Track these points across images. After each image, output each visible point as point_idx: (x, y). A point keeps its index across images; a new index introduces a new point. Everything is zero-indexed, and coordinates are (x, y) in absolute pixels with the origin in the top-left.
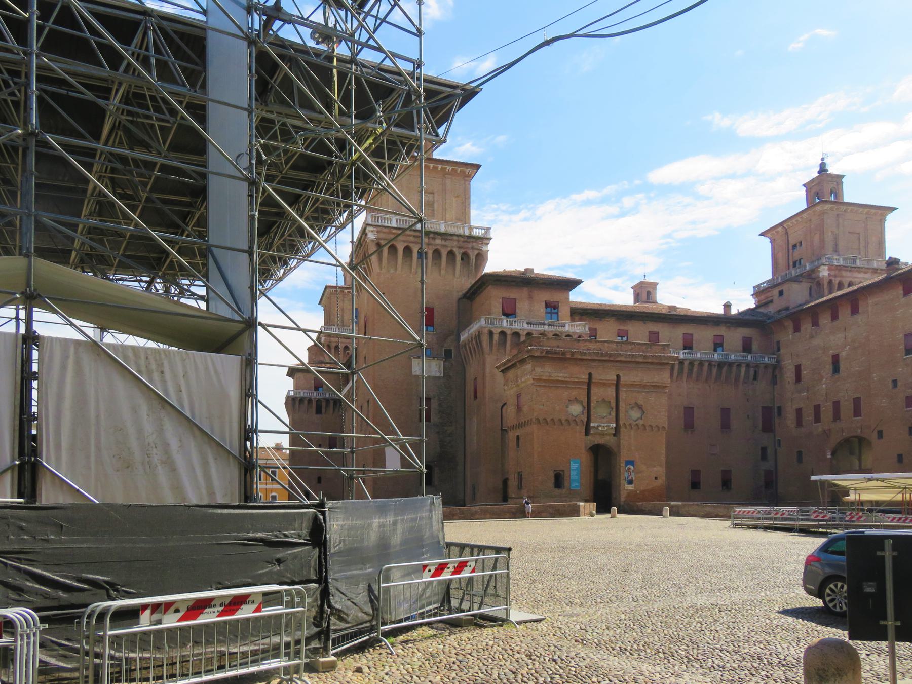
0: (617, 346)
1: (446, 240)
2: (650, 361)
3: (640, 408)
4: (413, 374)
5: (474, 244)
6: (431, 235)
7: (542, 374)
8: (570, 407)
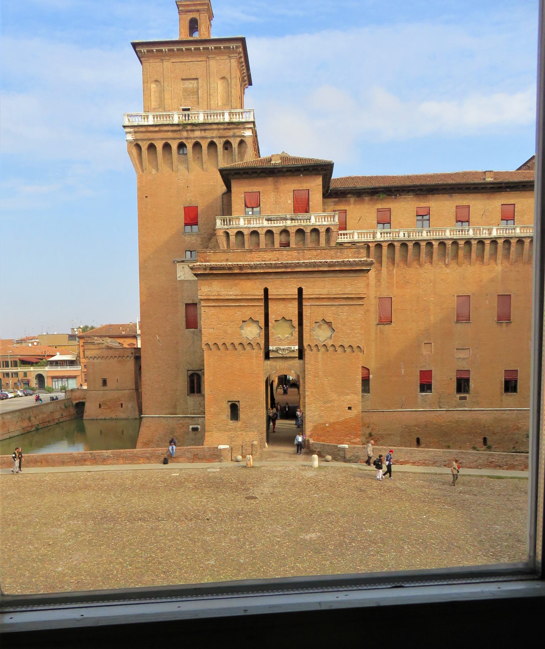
0: (298, 253)
1: (205, 130)
2: (337, 269)
3: (329, 324)
4: (178, 279)
5: (235, 131)
6: (189, 128)
7: (209, 293)
8: (245, 328)
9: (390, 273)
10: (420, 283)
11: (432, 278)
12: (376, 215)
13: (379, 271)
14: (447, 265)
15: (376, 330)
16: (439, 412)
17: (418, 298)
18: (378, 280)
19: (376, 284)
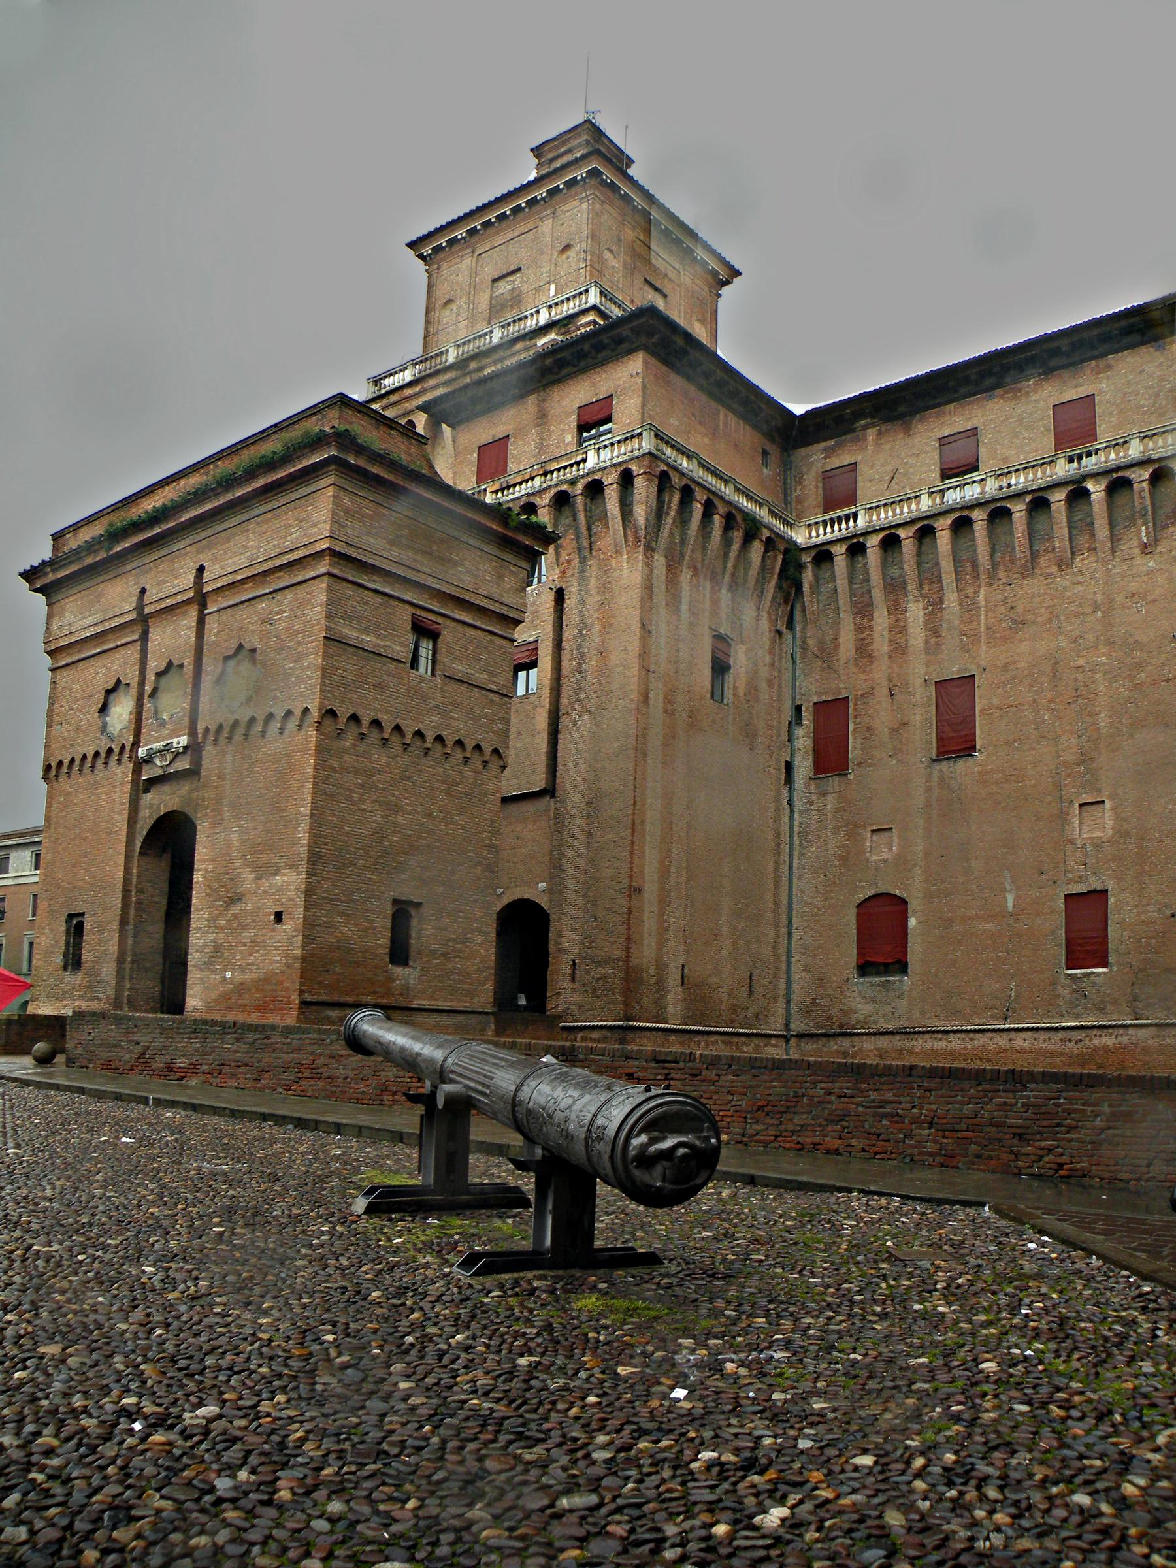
9: (968, 606)
10: (1062, 618)
11: (1099, 598)
12: (937, 457)
13: (935, 605)
14: (1145, 546)
15: (929, 779)
16: (1131, 1031)
17: (1057, 663)
18: (933, 630)
19: (927, 642)
